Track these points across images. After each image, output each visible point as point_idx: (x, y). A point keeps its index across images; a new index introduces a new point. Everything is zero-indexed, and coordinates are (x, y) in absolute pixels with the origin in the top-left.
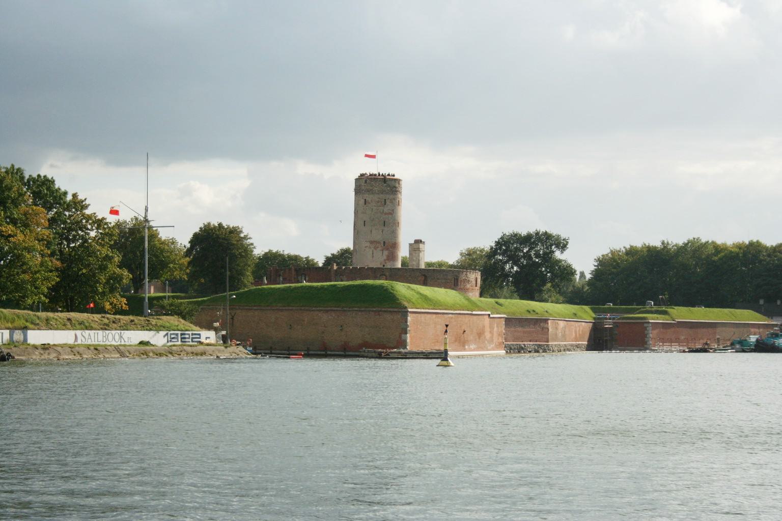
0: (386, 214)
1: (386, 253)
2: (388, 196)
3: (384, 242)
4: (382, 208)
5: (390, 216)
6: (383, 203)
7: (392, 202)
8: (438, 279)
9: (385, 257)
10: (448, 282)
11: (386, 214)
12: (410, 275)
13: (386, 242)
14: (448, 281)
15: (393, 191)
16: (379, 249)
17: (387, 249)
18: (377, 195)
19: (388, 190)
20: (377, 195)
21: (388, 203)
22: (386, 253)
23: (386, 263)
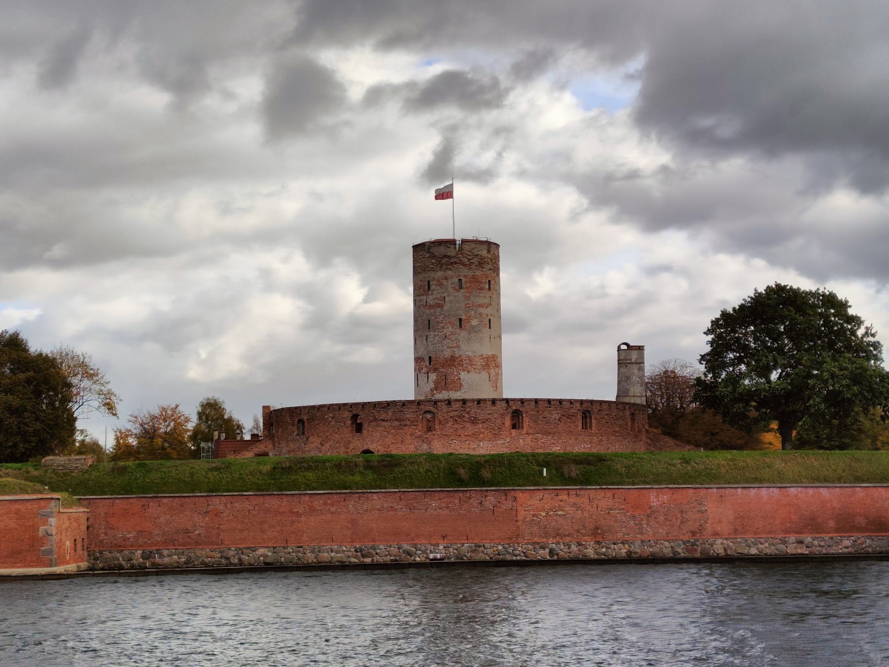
0: (431, 307)
1: (433, 376)
2: (432, 274)
3: (430, 358)
4: (424, 298)
5: (439, 310)
6: (426, 287)
7: (440, 285)
8: (383, 420)
9: (432, 385)
10: (405, 425)
11: (431, 307)
12: (333, 418)
13: (433, 356)
14: (408, 423)
15: (442, 265)
16: (424, 370)
17: (435, 370)
18: (454, 275)
19: (432, 264)
20: (454, 275)
21: (433, 287)
22: (433, 376)
23: (433, 395)
